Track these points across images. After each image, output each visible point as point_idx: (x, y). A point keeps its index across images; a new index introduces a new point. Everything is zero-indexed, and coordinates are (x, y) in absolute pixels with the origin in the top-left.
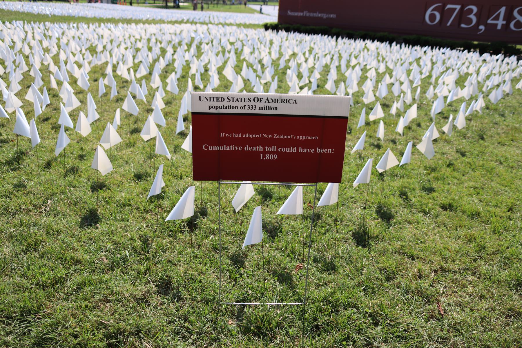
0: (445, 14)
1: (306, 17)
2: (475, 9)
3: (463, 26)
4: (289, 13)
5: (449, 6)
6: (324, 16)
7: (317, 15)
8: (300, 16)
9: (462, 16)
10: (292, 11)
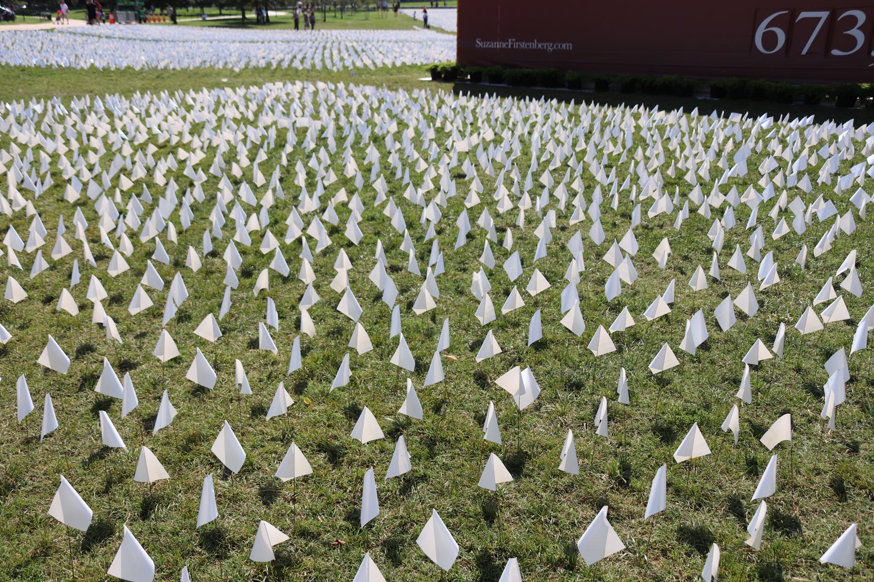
0: (796, 31)
2: (861, 16)
3: (836, 52)
4: (479, 44)
5: (804, 15)
6: (550, 47)
7: (536, 45)
8: (501, 49)
9: (834, 32)
10: (482, 41)
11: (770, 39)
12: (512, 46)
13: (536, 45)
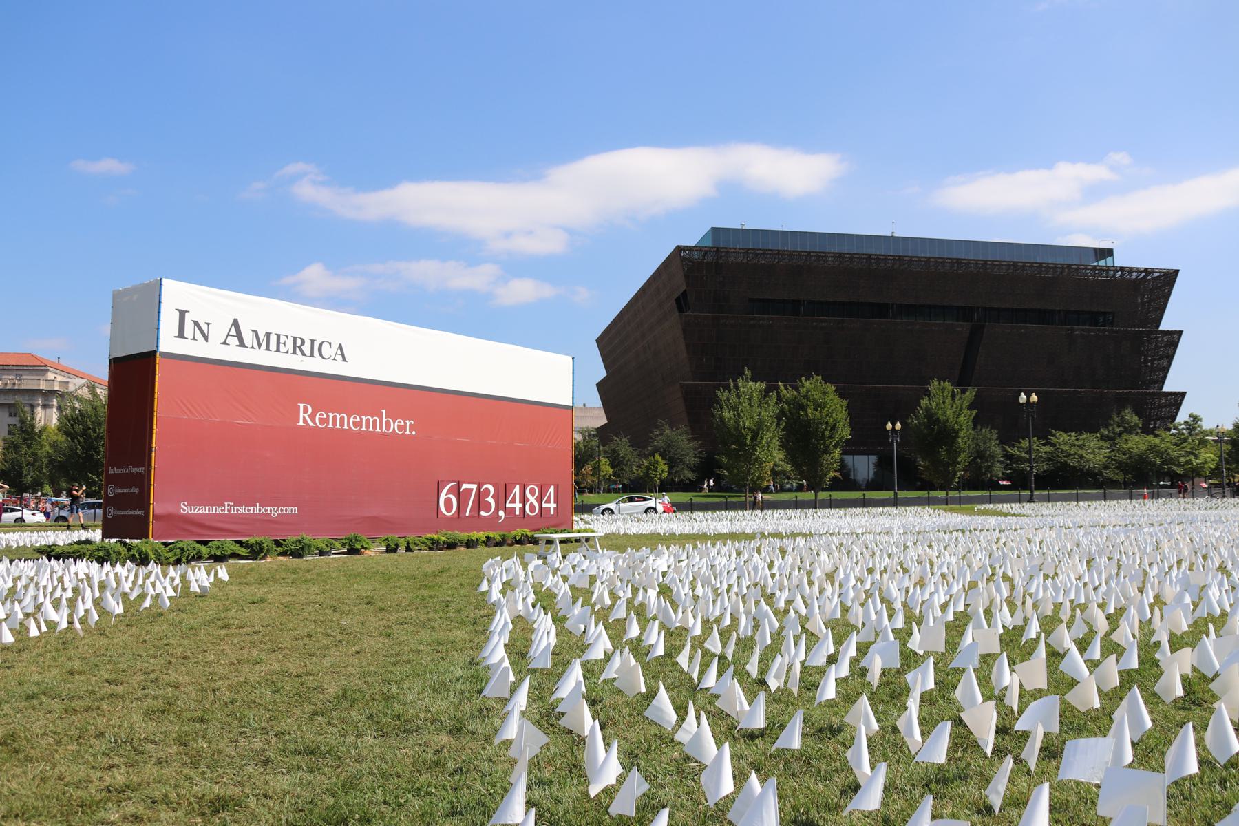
1: (229, 516)
3: (483, 513)
5: (465, 486)
6: (274, 511)
7: (258, 510)
10: (190, 504)
11: (448, 503)
12: (229, 511)
13: (258, 510)
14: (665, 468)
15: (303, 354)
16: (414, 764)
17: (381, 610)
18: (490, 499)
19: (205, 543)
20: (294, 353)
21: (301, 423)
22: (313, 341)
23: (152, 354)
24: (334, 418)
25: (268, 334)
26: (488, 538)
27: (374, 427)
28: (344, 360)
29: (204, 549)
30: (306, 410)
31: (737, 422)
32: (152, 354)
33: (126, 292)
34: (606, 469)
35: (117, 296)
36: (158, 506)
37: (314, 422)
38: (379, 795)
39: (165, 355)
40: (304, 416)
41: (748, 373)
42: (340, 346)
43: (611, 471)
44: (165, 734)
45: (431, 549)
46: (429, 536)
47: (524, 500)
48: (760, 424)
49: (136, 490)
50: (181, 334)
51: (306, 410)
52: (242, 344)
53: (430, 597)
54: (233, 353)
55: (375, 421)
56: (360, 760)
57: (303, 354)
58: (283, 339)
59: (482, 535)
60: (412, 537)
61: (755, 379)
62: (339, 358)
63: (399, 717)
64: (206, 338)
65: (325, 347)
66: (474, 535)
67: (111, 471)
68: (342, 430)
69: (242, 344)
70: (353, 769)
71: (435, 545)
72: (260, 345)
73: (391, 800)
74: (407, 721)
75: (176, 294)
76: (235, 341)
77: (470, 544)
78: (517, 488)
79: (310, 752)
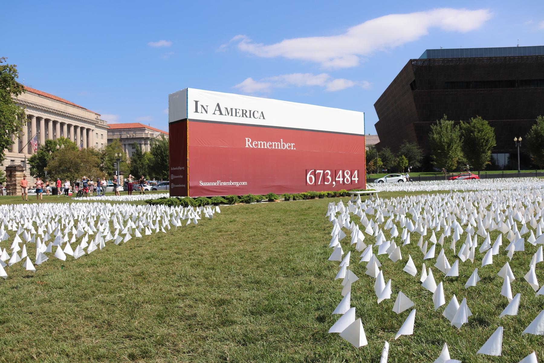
0: (316, 176)
1: (219, 186)
3: (326, 183)
5: (318, 171)
6: (237, 184)
7: (231, 183)
11: (311, 179)
13: (231, 183)
14: (407, 161)
15: (246, 117)
16: (301, 288)
17: (284, 224)
18: (329, 177)
19: (210, 198)
20: (243, 116)
21: (247, 146)
22: (250, 111)
23: (185, 120)
24: (261, 144)
25: (232, 109)
26: (328, 194)
27: (278, 147)
28: (264, 118)
29: (210, 200)
30: (249, 141)
31: (440, 140)
32: (186, 120)
33: (174, 95)
34: (380, 163)
35: (171, 97)
36: (191, 183)
37: (252, 145)
38: (287, 301)
39: (190, 120)
40: (249, 143)
41: (445, 117)
42: (262, 112)
43: (382, 163)
44: (199, 274)
45: (304, 199)
46: (303, 193)
47: (344, 177)
48: (451, 140)
49: (182, 177)
50: (196, 111)
51: (249, 141)
52: (221, 114)
53: (305, 219)
54: (218, 118)
55: (278, 144)
56: (278, 286)
57: (246, 117)
58: (238, 111)
59: (326, 193)
60: (295, 194)
61: (449, 119)
62: (262, 118)
63: (293, 269)
64: (206, 112)
65: (256, 113)
66: (322, 193)
67: (172, 169)
68: (264, 149)
69: (221, 114)
70: (276, 290)
71: (305, 197)
72: (228, 114)
73: (292, 303)
74: (297, 271)
75: (194, 94)
76: (218, 112)
77: (321, 196)
78: (341, 172)
79: (257, 282)
